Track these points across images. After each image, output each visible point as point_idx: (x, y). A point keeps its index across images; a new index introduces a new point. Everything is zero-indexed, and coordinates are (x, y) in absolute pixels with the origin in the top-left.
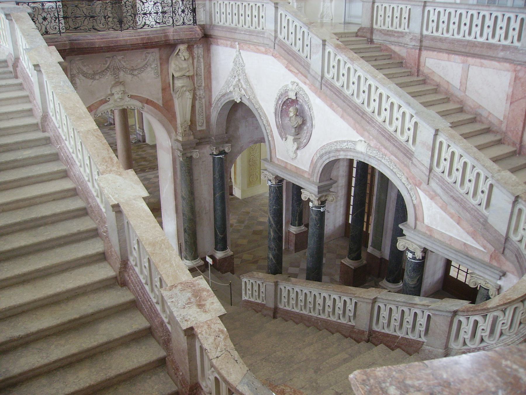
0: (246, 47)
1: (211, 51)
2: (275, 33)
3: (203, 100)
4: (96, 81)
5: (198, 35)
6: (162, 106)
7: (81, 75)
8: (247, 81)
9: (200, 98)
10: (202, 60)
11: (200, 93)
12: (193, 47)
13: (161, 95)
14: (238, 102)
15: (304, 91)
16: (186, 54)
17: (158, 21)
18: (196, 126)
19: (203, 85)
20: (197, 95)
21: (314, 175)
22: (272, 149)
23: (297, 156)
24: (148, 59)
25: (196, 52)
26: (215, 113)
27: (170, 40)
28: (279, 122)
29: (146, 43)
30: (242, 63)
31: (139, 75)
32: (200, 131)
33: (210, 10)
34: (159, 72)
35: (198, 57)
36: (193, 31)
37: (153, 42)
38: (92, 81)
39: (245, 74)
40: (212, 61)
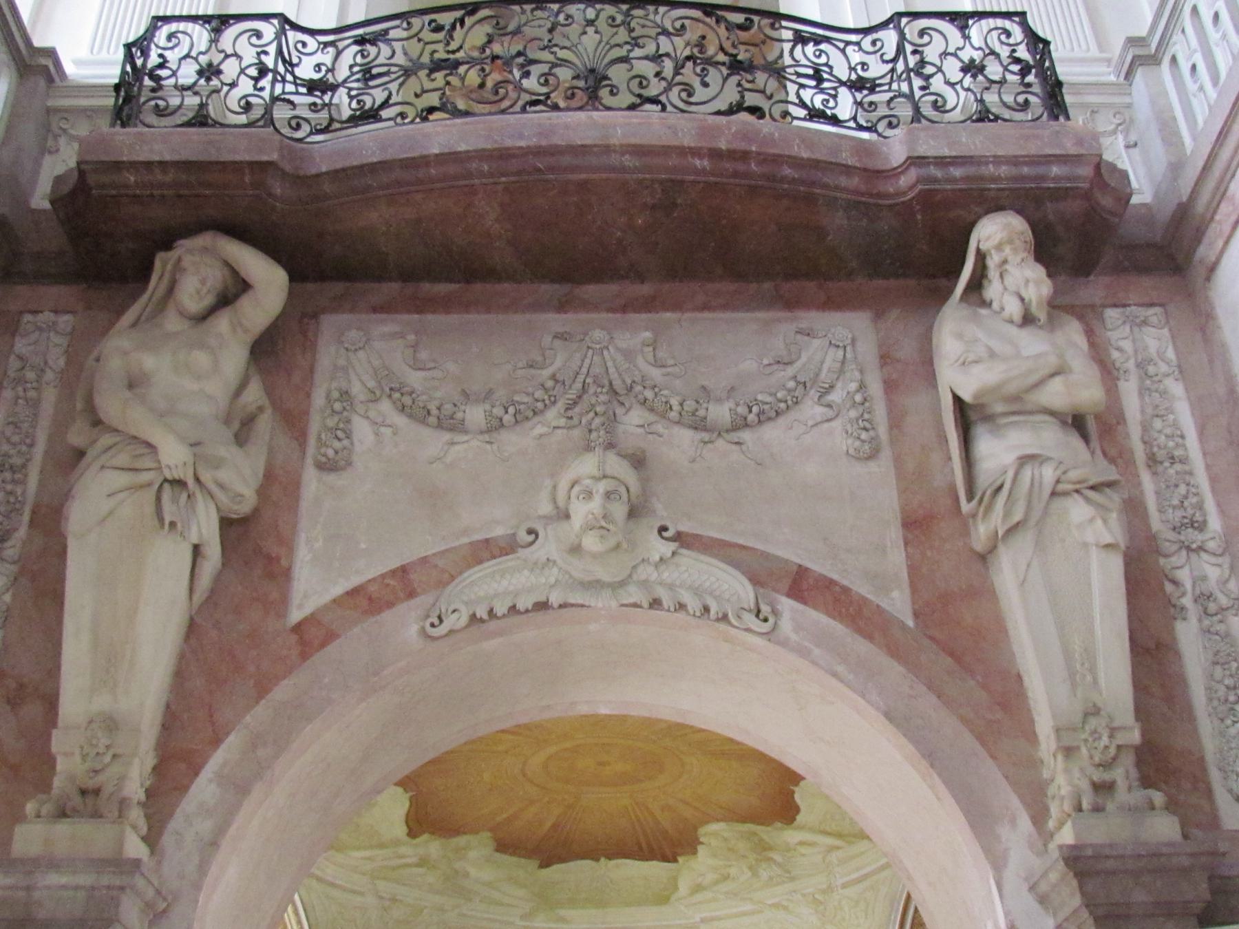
4: (466, 448)
6: (910, 623)
7: (386, 406)
9: (1203, 598)
10: (1176, 388)
13: (897, 559)
18: (1209, 793)
19: (1215, 524)
20: (1175, 582)
24: (804, 359)
25: (1127, 345)
27: (895, 173)
29: (732, 155)
31: (746, 435)
34: (882, 430)
37: (777, 159)
38: (447, 436)
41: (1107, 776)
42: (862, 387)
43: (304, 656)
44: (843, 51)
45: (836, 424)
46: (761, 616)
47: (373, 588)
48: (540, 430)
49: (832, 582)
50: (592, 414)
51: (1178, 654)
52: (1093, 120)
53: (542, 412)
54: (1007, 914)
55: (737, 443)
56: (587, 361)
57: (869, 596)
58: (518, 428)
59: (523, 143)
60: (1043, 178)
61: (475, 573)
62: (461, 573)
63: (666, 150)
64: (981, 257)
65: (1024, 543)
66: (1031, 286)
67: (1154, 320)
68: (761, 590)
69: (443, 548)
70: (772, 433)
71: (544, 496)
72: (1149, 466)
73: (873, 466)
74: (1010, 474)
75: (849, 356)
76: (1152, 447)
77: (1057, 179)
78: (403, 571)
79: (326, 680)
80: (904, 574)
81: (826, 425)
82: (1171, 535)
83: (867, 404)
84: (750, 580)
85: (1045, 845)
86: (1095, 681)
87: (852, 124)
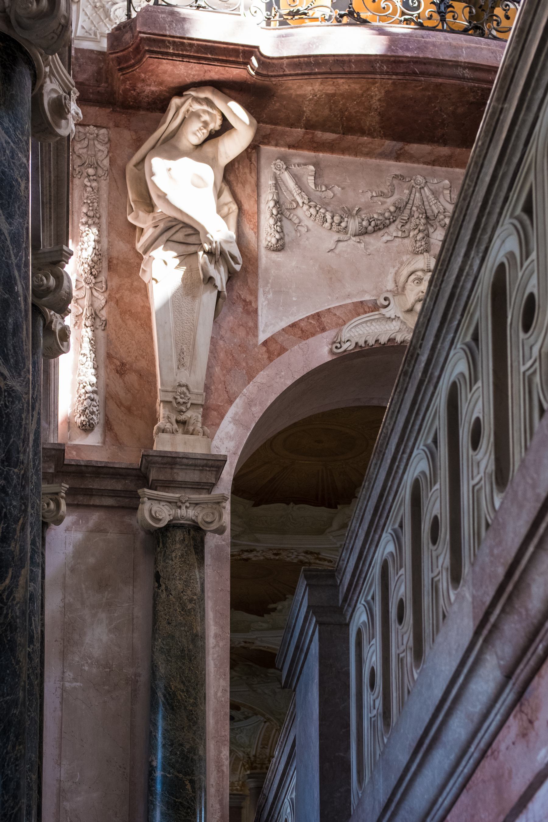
43: (270, 359)
47: (302, 324)
48: (386, 238)
50: (417, 231)
53: (388, 226)
56: (412, 196)
58: (374, 235)
59: (408, 54)
61: (357, 320)
62: (349, 320)
69: (337, 305)
71: (390, 277)
78: (318, 316)
79: (283, 373)
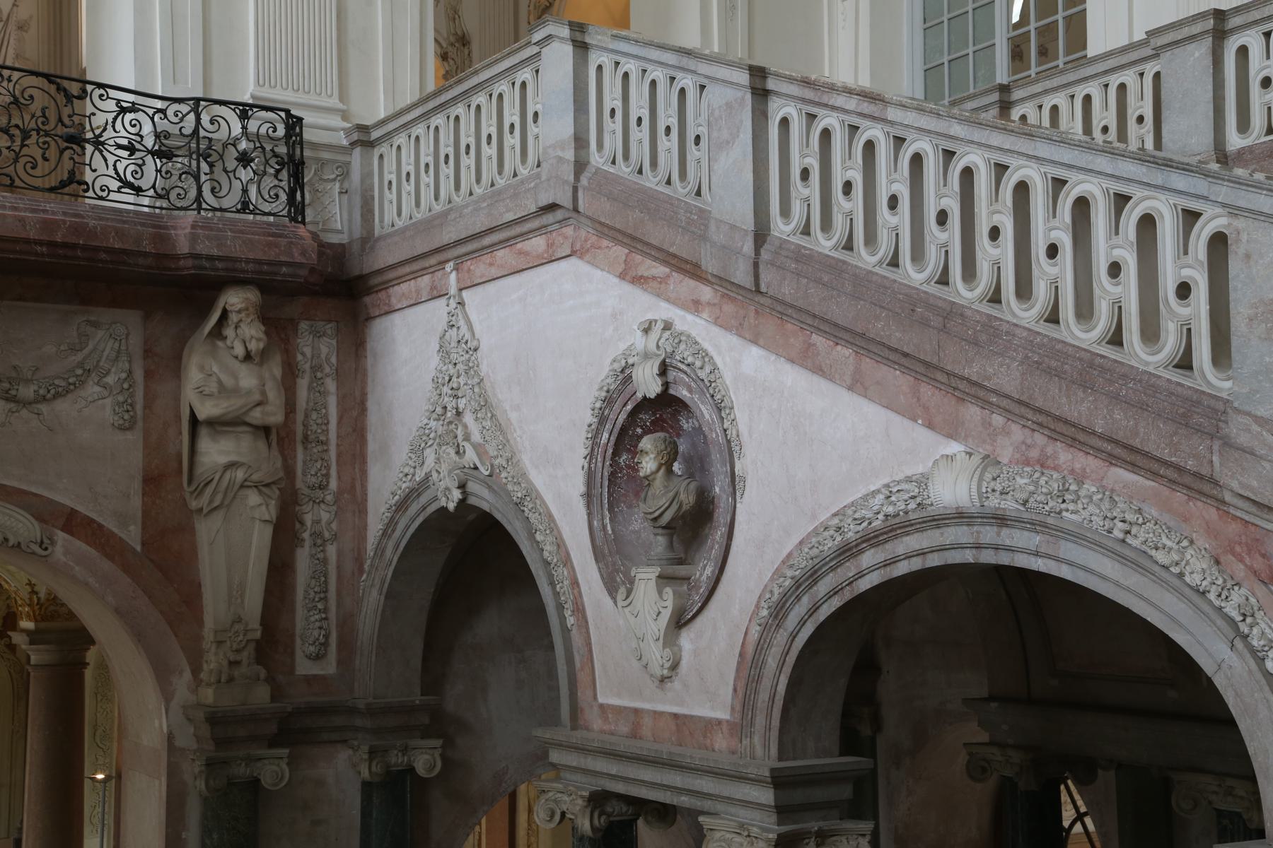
0: (479, 268)
1: (369, 346)
2: (576, 149)
3: (332, 550)
5: (303, 253)
6: (139, 548)
8: (485, 406)
9: (316, 535)
10: (331, 385)
11: (316, 516)
12: (296, 330)
13: (136, 502)
14: (451, 506)
15: (696, 343)
16: (253, 332)
17: (130, 178)
18: (292, 654)
19: (333, 484)
20: (302, 523)
21: (752, 724)
22: (578, 665)
23: (675, 666)
24: (90, 346)
25: (308, 351)
26: (375, 593)
27: (177, 257)
28: (604, 527)
29: (65, 245)
30: (468, 336)
31: (43, 408)
32: (310, 680)
33: (362, 181)
35: (316, 368)
36: (280, 236)
37: (97, 249)
39: (476, 380)
40: (369, 389)
41: (238, 658)
42: (130, 372)
44: (152, 119)
45: (108, 401)
46: (44, 546)
49: (93, 521)
51: (294, 571)
52: (321, 169)
54: (168, 726)
55: (38, 414)
57: (115, 530)
60: (276, 274)
63: (15, 240)
64: (225, 314)
65: (217, 520)
66: (254, 341)
67: (329, 332)
68: (45, 526)
70: (62, 406)
72: (303, 443)
73: (129, 436)
74: (217, 478)
75: (123, 348)
76: (307, 430)
77: (284, 275)
80: (139, 514)
81: (100, 402)
82: (306, 491)
83: (131, 390)
84: (37, 519)
85: (197, 687)
86: (243, 602)
87: (151, 192)
